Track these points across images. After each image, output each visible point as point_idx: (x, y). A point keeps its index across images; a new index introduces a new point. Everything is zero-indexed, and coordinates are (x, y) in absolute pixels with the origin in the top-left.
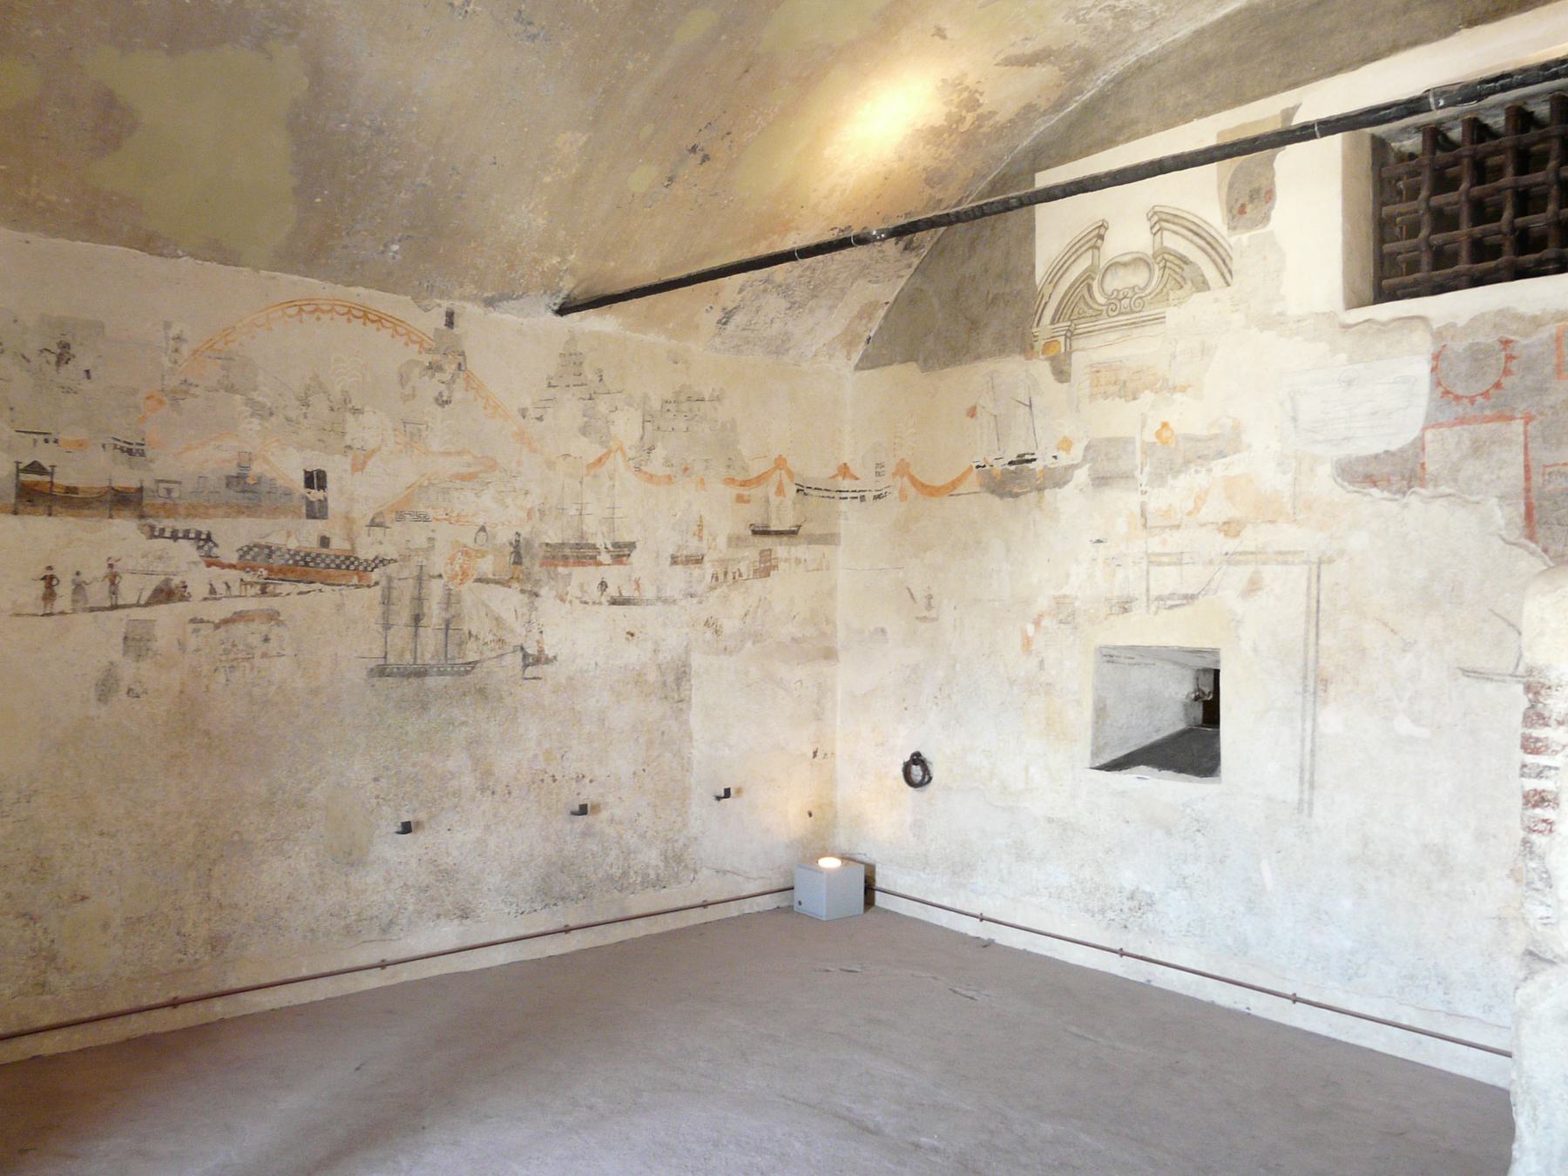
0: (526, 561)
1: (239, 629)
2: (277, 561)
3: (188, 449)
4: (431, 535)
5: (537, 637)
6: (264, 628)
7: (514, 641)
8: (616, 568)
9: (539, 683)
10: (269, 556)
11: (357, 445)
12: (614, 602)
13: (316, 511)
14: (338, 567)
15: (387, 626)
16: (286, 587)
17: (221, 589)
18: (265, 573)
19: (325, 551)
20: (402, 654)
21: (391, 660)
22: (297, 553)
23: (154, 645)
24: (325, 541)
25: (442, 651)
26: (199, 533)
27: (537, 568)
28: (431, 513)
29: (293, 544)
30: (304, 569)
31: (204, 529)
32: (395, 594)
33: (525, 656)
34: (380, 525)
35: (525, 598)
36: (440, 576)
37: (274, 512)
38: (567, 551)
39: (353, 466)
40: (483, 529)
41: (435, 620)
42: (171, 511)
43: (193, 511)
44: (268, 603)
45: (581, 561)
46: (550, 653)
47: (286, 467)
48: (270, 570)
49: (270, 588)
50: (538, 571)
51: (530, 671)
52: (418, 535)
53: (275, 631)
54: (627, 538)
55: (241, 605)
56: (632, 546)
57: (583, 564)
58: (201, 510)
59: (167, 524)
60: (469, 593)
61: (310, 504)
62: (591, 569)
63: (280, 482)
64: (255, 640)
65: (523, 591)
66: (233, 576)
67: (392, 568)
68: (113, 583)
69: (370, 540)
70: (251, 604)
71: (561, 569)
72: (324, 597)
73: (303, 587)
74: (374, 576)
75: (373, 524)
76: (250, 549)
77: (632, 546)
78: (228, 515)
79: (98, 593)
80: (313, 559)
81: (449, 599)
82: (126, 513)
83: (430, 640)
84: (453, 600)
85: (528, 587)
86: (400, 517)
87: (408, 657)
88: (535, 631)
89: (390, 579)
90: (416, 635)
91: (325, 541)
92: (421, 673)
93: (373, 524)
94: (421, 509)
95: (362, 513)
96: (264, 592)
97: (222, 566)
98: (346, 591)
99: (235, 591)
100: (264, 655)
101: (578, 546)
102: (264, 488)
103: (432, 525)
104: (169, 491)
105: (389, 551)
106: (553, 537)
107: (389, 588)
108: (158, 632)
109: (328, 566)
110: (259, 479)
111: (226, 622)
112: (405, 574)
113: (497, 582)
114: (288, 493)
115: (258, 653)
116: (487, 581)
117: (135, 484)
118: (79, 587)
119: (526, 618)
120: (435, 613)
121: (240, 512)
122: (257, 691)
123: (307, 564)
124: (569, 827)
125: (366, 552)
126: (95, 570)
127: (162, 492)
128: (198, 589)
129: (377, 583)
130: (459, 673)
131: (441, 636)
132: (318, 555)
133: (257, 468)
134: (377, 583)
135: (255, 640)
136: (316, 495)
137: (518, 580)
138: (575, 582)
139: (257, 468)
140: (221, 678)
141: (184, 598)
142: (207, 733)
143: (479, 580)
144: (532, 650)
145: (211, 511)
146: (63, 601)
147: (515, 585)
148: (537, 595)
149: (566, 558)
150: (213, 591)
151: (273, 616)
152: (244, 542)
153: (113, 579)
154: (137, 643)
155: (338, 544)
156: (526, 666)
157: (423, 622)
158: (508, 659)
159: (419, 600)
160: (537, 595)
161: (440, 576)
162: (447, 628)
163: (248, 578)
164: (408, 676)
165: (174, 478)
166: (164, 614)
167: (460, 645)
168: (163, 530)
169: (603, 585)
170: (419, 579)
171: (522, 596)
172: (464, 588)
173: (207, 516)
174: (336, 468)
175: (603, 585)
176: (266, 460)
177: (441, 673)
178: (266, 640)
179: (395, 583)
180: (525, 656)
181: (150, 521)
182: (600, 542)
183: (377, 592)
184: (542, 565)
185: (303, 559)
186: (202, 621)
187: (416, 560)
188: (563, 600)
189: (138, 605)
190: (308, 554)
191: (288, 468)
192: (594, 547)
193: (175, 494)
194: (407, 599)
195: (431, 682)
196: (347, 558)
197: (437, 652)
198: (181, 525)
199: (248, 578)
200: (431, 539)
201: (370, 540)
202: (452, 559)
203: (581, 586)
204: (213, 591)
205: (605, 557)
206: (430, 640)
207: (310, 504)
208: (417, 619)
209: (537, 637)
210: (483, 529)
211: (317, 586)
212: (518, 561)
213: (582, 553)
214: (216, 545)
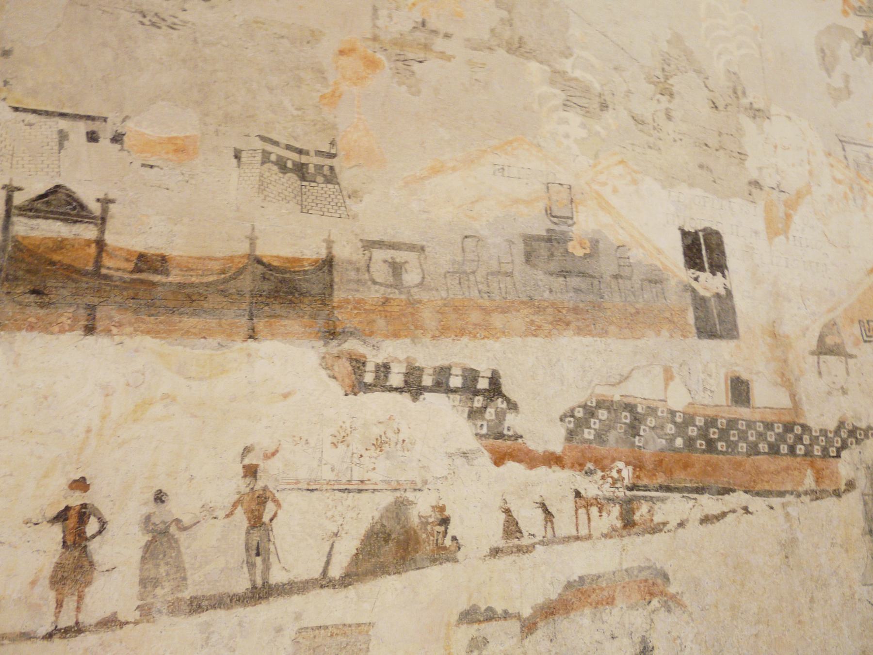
2: (651, 442)
3: (436, 171)
6: (638, 619)
10: (633, 429)
11: (768, 181)
13: (715, 321)
14: (774, 450)
16: (673, 508)
18: (627, 473)
19: (743, 412)
22: (689, 420)
24: (740, 390)
26: (471, 376)
29: (678, 400)
31: (484, 368)
34: (835, 351)
37: (634, 321)
42: (402, 319)
43: (455, 321)
44: (642, 550)
47: (644, 222)
48: (638, 466)
58: (475, 316)
59: (395, 352)
61: (700, 303)
70: (603, 556)
73: (709, 504)
75: (824, 349)
76: (590, 412)
78: (534, 330)
80: (724, 434)
82: (293, 325)
91: (740, 390)
93: (824, 349)
95: (802, 324)
96: (628, 523)
97: (531, 460)
98: (797, 507)
102: (606, 266)
104: (396, 268)
109: (753, 450)
110: (595, 243)
111: (550, 611)
114: (655, 280)
117: (311, 250)
121: (561, 323)
123: (711, 446)
127: (381, 272)
132: (732, 423)
145: (497, 320)
152: (574, 398)
155: (767, 396)
163: (591, 488)
165: (406, 235)
168: (384, 369)
173: (487, 331)
176: (605, 206)
181: (352, 345)
185: (703, 433)
190: (711, 422)
191: (640, 218)
193: (411, 277)
196: (788, 428)
199: (591, 488)
214: (513, 406)
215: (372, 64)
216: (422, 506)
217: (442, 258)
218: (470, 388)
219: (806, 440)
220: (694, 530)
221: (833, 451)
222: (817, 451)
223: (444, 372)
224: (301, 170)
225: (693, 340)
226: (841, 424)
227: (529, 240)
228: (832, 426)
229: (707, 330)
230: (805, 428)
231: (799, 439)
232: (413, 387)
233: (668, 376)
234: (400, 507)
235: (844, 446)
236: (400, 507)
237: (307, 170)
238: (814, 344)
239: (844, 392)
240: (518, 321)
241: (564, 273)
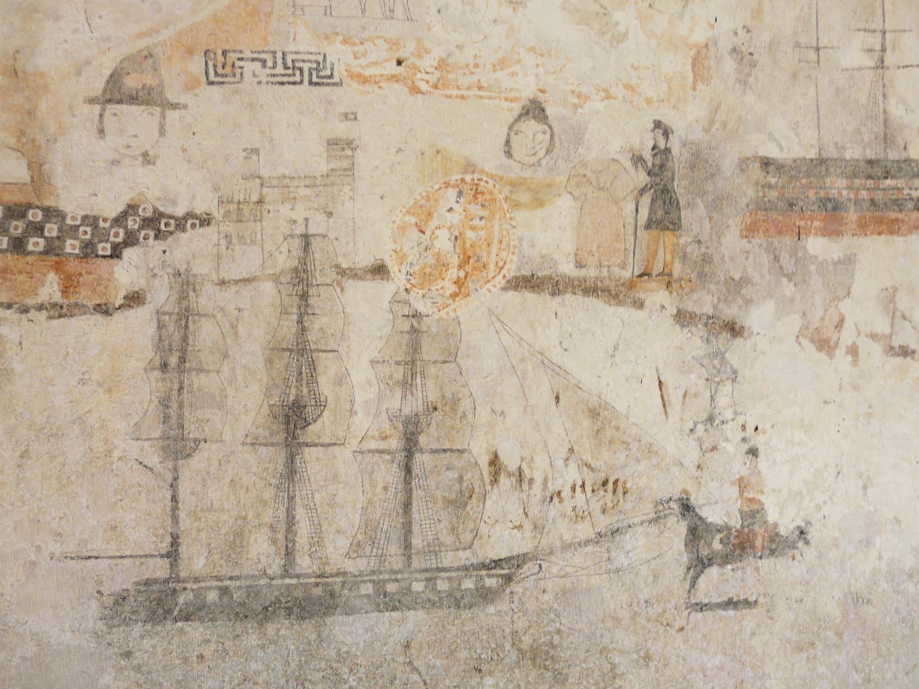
0: (694, 216)
5: (739, 467)
7: (653, 483)
9: (749, 619)
15: (178, 446)
20: (237, 541)
21: (196, 560)
25: (390, 525)
27: (732, 240)
32: (205, 334)
33: (697, 531)
36: (380, 270)
41: (362, 422)
46: (781, 516)
50: (735, 249)
51: (716, 582)
60: (489, 328)
67: (189, 246)
69: (104, 149)
74: (127, 272)
75: (115, 93)
81: (414, 349)
83: (346, 490)
84: (429, 350)
85: (704, 302)
87: (262, 551)
88: (732, 448)
89: (185, 284)
90: (291, 472)
93: (115, 93)
105: (176, 185)
106: (788, 138)
107: (185, 316)
112: (247, 261)
113: (591, 289)
116: (555, 286)
119: (699, 408)
120: (359, 391)
125: (90, 182)
129: (135, 299)
130: (456, 601)
131: (388, 474)
134: (135, 299)
137: (668, 280)
138: (866, 284)
143: (527, 283)
144: (721, 509)
147: (657, 296)
149: (832, 209)
156: (700, 564)
157: (318, 429)
158: (638, 545)
159: (300, 354)
160: (734, 329)
161: (380, 270)
170: (301, 283)
172: (470, 311)
179: (206, 299)
180: (697, 531)
183: (137, 326)
184: (750, 231)
187: (283, 217)
194: (251, 351)
200: (340, 146)
201: (104, 149)
206: (346, 490)
208: (294, 420)
209: (739, 467)
212: (664, 211)
219: (52, 230)
221: (104, 248)
222: (71, 246)
226: (131, 208)
228: (112, 210)
230: (50, 213)
231: (38, 229)
235: (131, 240)
238: (98, 86)
239: (147, 159)
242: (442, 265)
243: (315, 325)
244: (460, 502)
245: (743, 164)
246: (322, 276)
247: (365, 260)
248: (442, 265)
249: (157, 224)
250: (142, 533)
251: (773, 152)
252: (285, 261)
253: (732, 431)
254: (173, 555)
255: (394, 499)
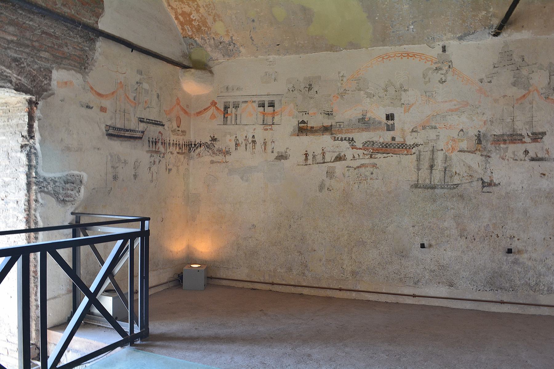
0: (484, 142)
1: (363, 170)
4: (438, 134)
8: (533, 144)
12: (533, 159)
13: (390, 128)
14: (399, 148)
15: (419, 169)
17: (356, 156)
19: (394, 142)
20: (425, 180)
21: (420, 182)
23: (335, 175)
24: (393, 139)
25: (443, 179)
27: (489, 145)
28: (438, 125)
30: (385, 148)
32: (422, 157)
35: (483, 158)
36: (442, 150)
37: (375, 129)
38: (506, 138)
39: (405, 110)
40: (462, 130)
45: (513, 141)
47: (379, 114)
48: (373, 150)
49: (373, 156)
50: (489, 146)
52: (432, 134)
53: (375, 171)
54: (541, 130)
55: (363, 162)
56: (544, 134)
57: (514, 143)
59: (339, 136)
60: (455, 156)
61: (388, 126)
62: (520, 145)
63: (377, 119)
64: (368, 174)
65: (482, 155)
66: (360, 152)
68: (323, 155)
69: (411, 137)
71: (502, 146)
72: (393, 159)
73: (385, 155)
74: (413, 151)
75: (413, 131)
76: (366, 142)
77: (544, 134)
78: (359, 132)
79: (319, 158)
80: (389, 145)
81: (446, 158)
84: (448, 159)
85: (485, 153)
86: (424, 128)
87: (428, 181)
89: (420, 151)
90: (431, 173)
91: (393, 139)
92: (433, 187)
93: (413, 131)
94: (433, 124)
95: (408, 128)
98: (402, 156)
99: (361, 157)
100: (371, 179)
101: (511, 135)
103: (438, 130)
105: (419, 141)
106: (498, 131)
107: (420, 155)
108: (337, 170)
109: (395, 148)
112: (427, 149)
113: (469, 152)
114: (380, 123)
115: (369, 178)
116: (464, 151)
117: (330, 124)
118: (314, 157)
120: (439, 163)
122: (368, 191)
124: (505, 258)
125: (410, 141)
126: (319, 152)
128: (349, 157)
129: (414, 153)
131: (443, 173)
132: (391, 144)
133: (368, 115)
134: (414, 153)
135: (368, 174)
136: (390, 122)
137: (479, 150)
139: (368, 115)
140: (356, 186)
141: (344, 160)
142: (351, 204)
143: (459, 151)
145: (353, 131)
146: (310, 161)
147: (478, 153)
148: (489, 157)
150: (354, 157)
151: (374, 165)
153: (324, 154)
154: (330, 174)
155: (399, 139)
159: (433, 159)
161: (442, 150)
162: (445, 170)
164: (428, 188)
166: (339, 165)
167: (451, 177)
169: (526, 152)
170: (433, 151)
171: (481, 157)
173: (352, 132)
174: (398, 112)
175: (526, 152)
177: (442, 188)
178: (372, 173)
182: (524, 133)
185: (385, 145)
186: (350, 167)
187: (431, 144)
188: (503, 159)
189: (331, 162)
192: (521, 135)
194: (427, 159)
195: (437, 191)
196: (402, 144)
197: (440, 179)
198: (344, 136)
201: (411, 137)
202: (447, 143)
203: (514, 153)
204: (354, 157)
205: (527, 140)
206: (437, 176)
207: (388, 126)
208: (432, 167)
210: (462, 130)
211: (391, 155)
212: (479, 141)
213: (515, 138)
215: (338, 97)
216: (342, 154)
217: (346, 123)
218: (349, 140)
220: (382, 159)
223: (346, 138)
224: (328, 114)
225: (386, 131)
227: (359, 119)
229: (388, 130)
232: (342, 140)
233: (380, 137)
234: (340, 154)
236: (340, 154)
237: (329, 114)
240: (356, 131)
241: (364, 123)
242: (450, 149)
243: (434, 156)
244: (451, 177)
245: (491, 135)
246: (435, 150)
247: (440, 149)
248: (450, 149)
249: (417, 145)
250: (414, 178)
251: (496, 134)
252: (431, 149)
253: (489, 170)
254: (418, 181)
255: (443, 176)
